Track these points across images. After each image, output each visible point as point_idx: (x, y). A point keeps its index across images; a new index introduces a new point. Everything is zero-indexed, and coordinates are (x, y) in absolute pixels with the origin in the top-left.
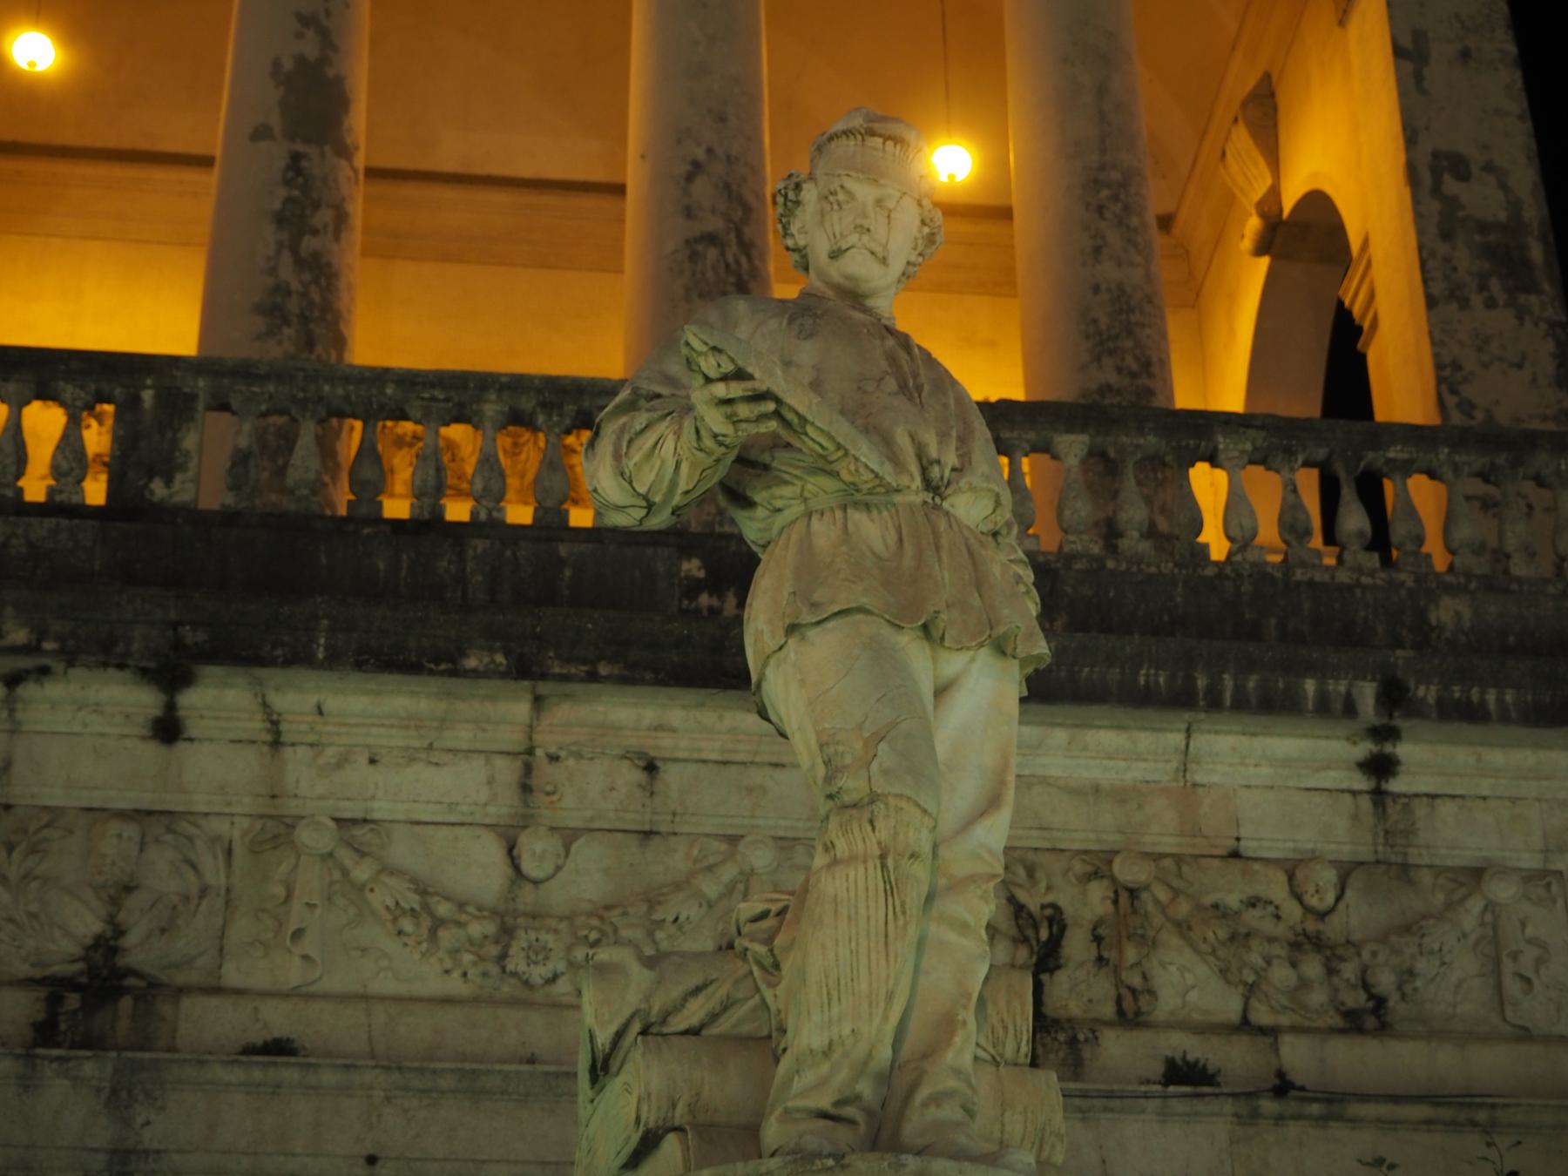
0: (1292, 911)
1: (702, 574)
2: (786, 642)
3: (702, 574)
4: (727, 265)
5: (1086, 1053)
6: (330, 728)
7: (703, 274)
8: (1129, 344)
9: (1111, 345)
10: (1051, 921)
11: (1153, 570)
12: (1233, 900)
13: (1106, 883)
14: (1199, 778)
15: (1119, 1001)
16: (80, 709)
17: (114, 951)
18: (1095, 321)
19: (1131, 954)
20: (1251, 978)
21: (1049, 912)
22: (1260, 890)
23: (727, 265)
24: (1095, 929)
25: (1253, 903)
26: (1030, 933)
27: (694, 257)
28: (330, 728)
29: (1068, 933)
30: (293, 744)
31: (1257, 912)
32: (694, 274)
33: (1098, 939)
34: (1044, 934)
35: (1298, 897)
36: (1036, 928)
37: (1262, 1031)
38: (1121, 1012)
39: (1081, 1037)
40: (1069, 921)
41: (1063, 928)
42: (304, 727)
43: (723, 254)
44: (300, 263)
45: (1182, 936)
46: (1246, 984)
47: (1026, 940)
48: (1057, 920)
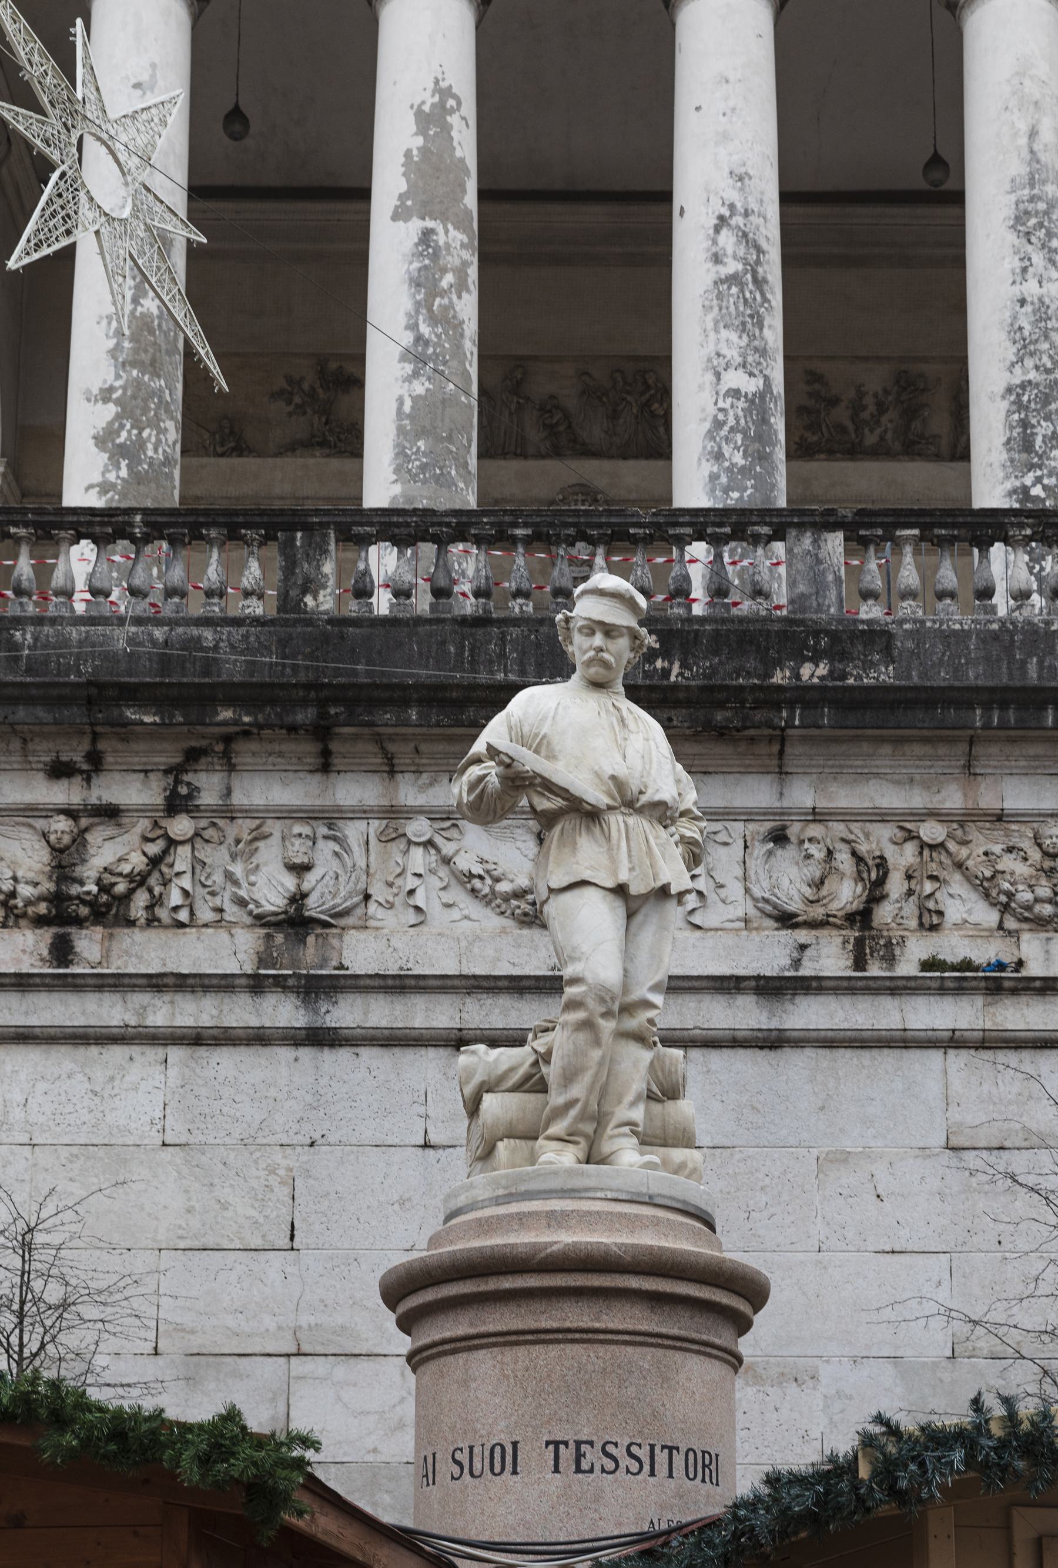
0: (1035, 855)
1: (657, 646)
2: (549, 898)
3: (657, 646)
4: (746, 300)
5: (897, 951)
6: (424, 761)
7: (727, 308)
8: (1045, 346)
9: (1032, 347)
10: (878, 866)
11: (957, 627)
12: (997, 849)
13: (916, 842)
14: (978, 771)
15: (920, 917)
16: (270, 755)
17: (300, 908)
18: (1021, 329)
19: (928, 887)
20: (1003, 899)
21: (878, 861)
22: (1015, 841)
23: (746, 300)
24: (907, 871)
25: (1010, 850)
26: (865, 875)
27: (720, 296)
28: (424, 761)
29: (890, 875)
30: (402, 772)
31: (1013, 856)
32: (720, 309)
33: (909, 877)
34: (874, 876)
35: (1039, 845)
36: (869, 872)
37: (1010, 933)
38: (921, 925)
39: (894, 941)
40: (891, 867)
41: (886, 874)
42: (407, 761)
43: (742, 291)
44: (433, 320)
45: (963, 874)
46: (1001, 903)
47: (863, 879)
48: (882, 863)
